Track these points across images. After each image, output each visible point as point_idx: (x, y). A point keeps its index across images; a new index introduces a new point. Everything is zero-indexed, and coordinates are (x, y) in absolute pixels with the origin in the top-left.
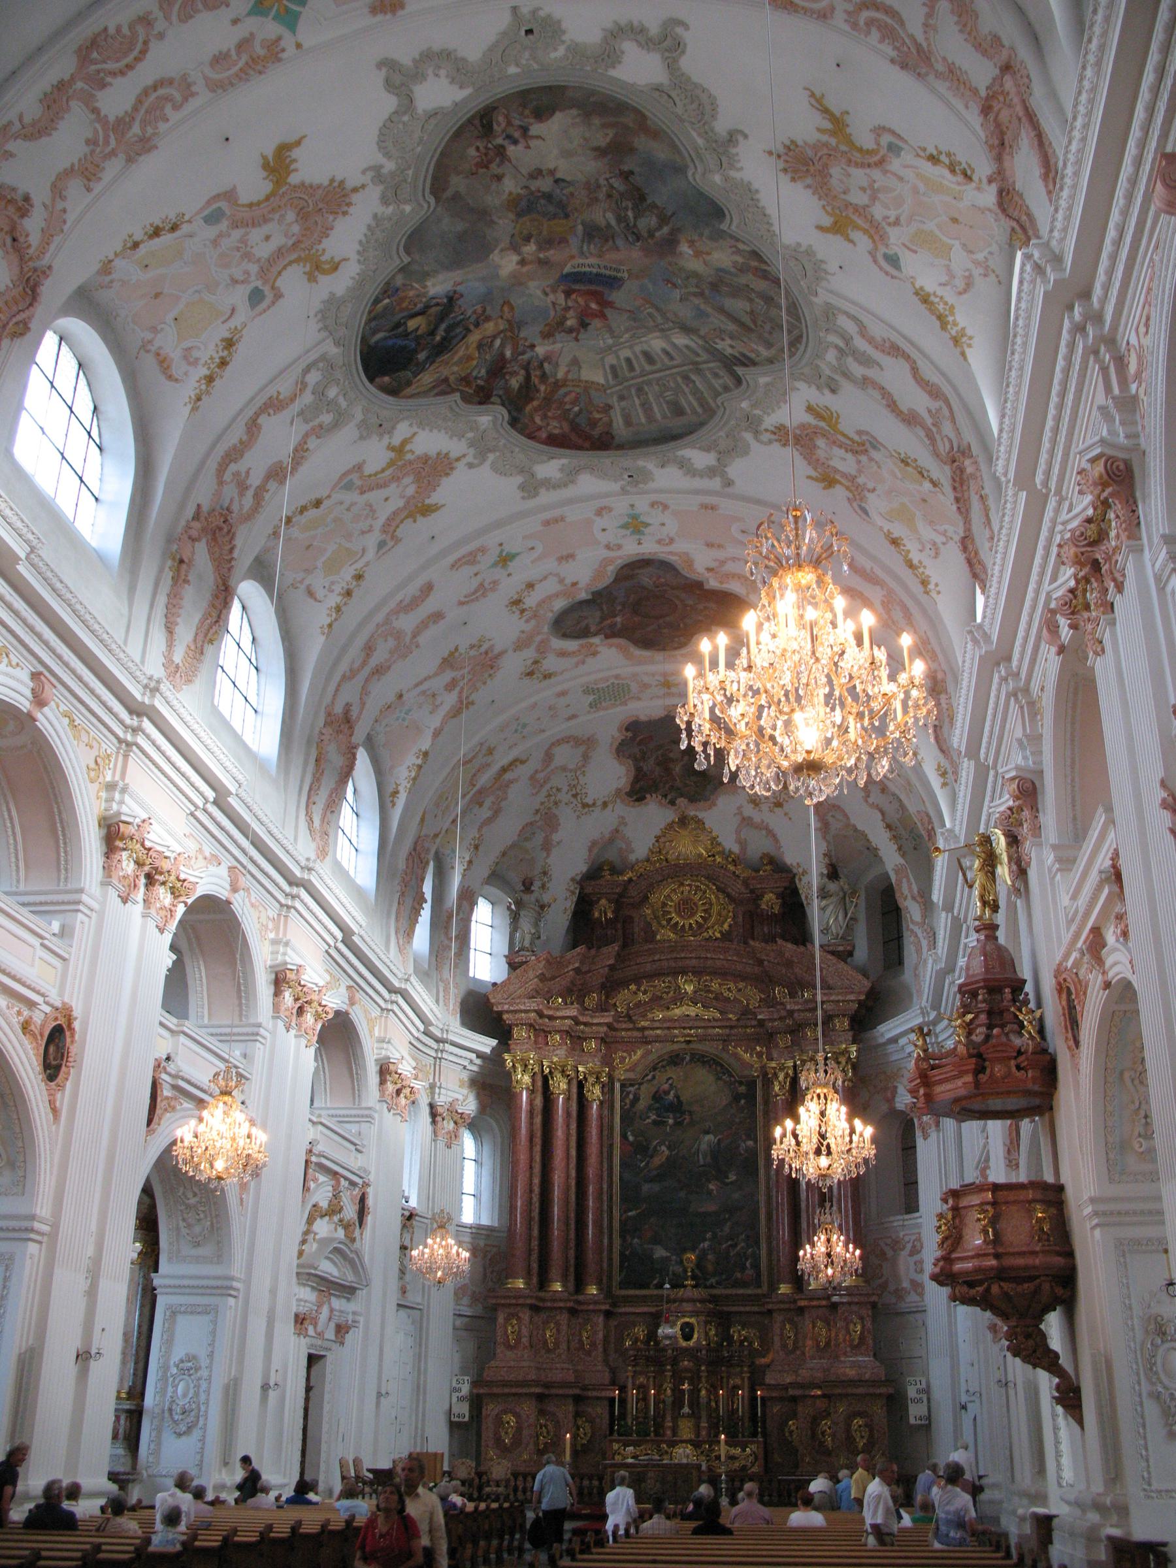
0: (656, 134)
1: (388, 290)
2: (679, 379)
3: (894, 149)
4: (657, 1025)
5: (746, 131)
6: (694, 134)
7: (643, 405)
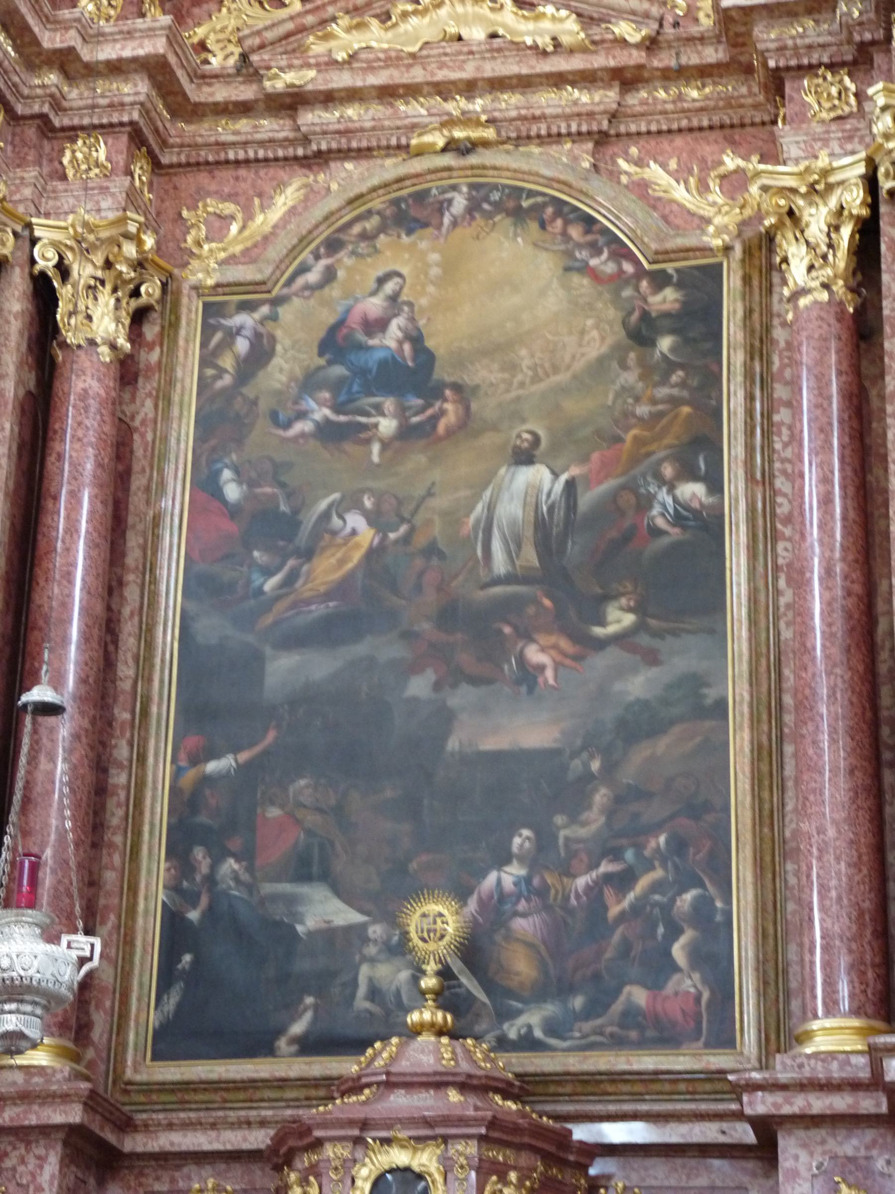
4: (342, 80)
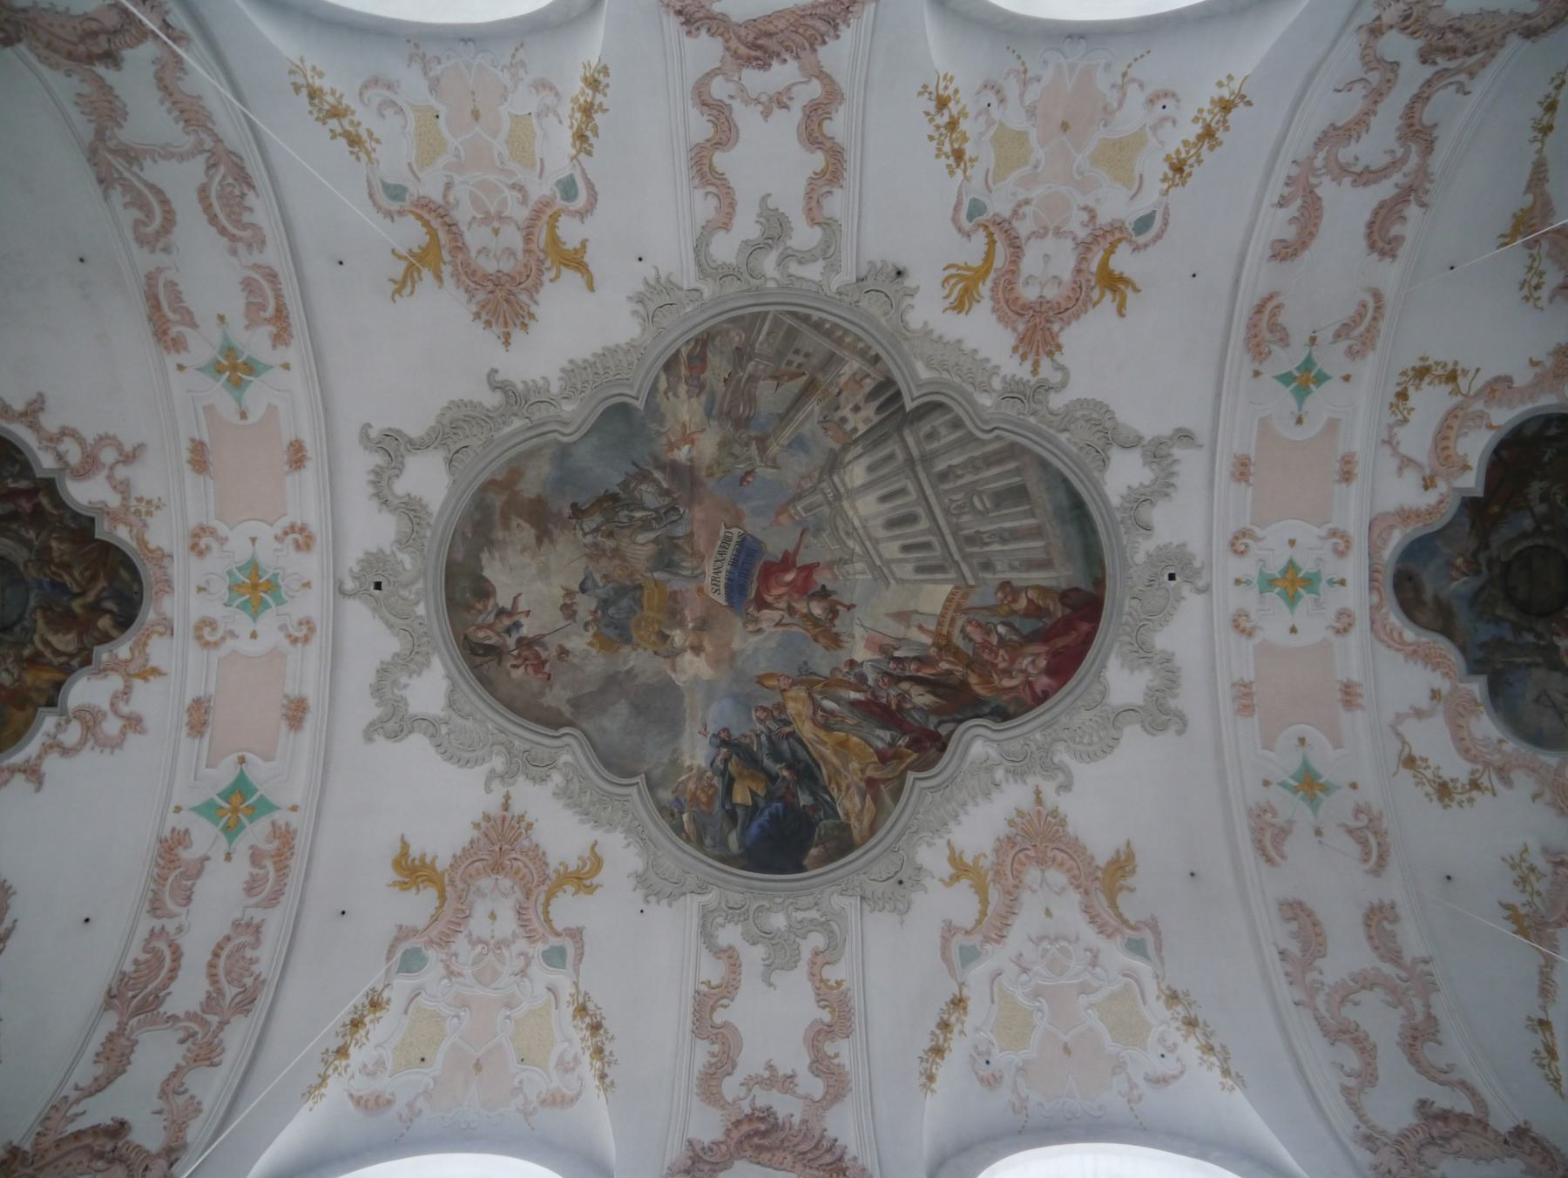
0: (514, 473)
1: (670, 813)
2: (946, 486)
3: (396, 192)
5: (487, 370)
6: (507, 430)
7: (1003, 541)
